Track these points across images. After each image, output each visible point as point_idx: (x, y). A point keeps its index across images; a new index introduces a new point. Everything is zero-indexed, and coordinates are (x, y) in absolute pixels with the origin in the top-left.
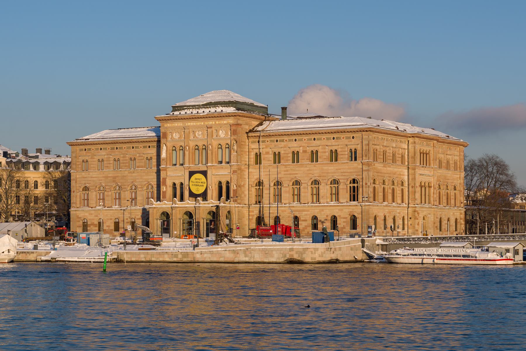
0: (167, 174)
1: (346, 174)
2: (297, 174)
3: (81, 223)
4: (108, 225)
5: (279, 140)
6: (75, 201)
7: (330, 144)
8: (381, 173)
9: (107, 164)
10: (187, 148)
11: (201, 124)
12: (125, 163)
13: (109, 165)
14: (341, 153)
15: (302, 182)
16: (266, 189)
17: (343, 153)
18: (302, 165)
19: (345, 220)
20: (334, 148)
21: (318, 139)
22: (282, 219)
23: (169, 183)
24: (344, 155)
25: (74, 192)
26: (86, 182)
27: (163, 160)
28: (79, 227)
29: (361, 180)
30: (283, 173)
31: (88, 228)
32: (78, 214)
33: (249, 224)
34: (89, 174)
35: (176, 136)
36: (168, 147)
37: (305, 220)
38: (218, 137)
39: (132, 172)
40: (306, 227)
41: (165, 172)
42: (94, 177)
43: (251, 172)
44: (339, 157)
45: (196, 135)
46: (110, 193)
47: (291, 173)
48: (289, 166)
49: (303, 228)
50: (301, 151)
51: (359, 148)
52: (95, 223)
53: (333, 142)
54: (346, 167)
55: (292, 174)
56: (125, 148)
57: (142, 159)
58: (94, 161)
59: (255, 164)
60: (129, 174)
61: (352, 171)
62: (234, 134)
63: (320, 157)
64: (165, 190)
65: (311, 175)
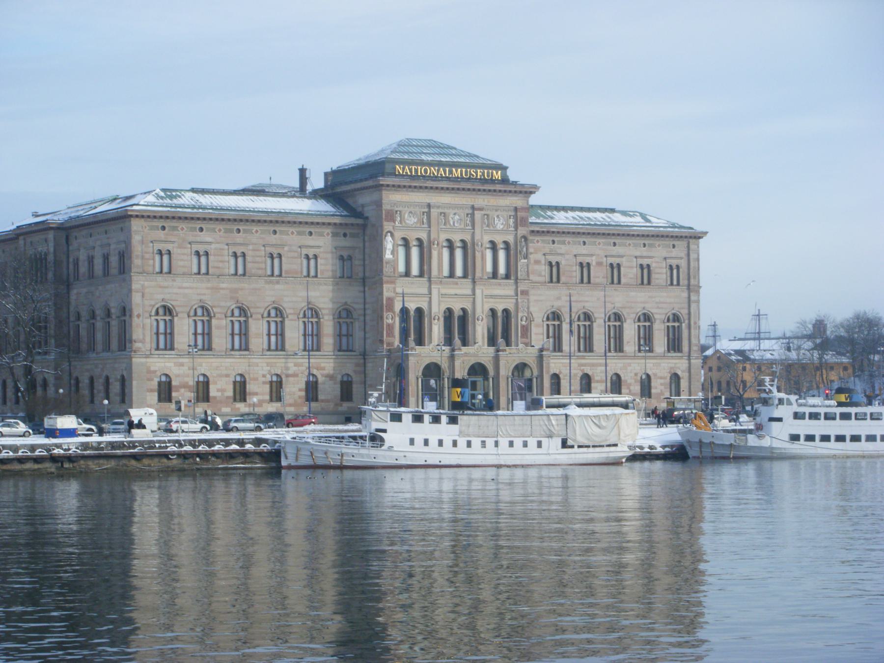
2: (587, 301)
3: (154, 384)
4: (219, 386)
6: (141, 337)
7: (638, 254)
13: (221, 265)
14: (657, 270)
15: (596, 315)
18: (597, 285)
19: (662, 381)
20: (645, 262)
23: (398, 307)
24: (660, 275)
25: (138, 316)
26: (167, 297)
27: (387, 263)
28: (152, 391)
29: (686, 317)
31: (174, 394)
35: (411, 221)
38: (492, 228)
41: (391, 286)
42: (185, 288)
44: (653, 276)
45: (449, 221)
46: (224, 322)
51: (683, 264)
53: (643, 251)
54: (665, 294)
55: (580, 301)
56: (257, 231)
57: (295, 258)
58: (184, 254)
60: (267, 286)
63: (624, 276)
64: (390, 321)
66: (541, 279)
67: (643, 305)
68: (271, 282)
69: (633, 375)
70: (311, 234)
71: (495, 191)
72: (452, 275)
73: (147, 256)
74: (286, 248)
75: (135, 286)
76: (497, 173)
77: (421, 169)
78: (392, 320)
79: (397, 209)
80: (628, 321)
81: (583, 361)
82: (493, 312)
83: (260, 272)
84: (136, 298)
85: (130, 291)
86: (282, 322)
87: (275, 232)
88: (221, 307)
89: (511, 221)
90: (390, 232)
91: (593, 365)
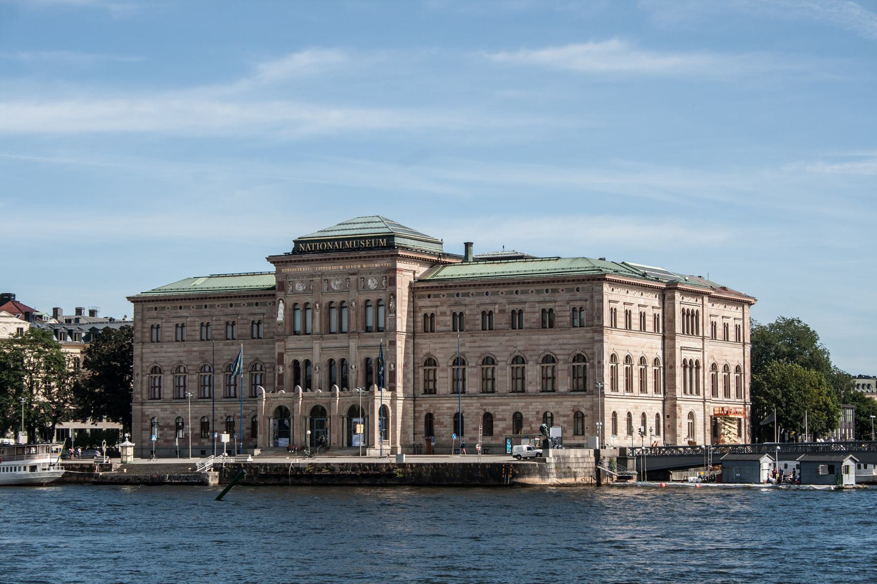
0: (285, 347)
1: (567, 347)
2: (490, 346)
5: (462, 293)
7: (541, 299)
8: (622, 345)
9: (191, 331)
10: (317, 305)
11: (339, 269)
12: (220, 330)
13: (193, 333)
14: (560, 314)
16: (443, 370)
17: (563, 314)
18: (499, 332)
20: (547, 306)
21: (523, 292)
22: (467, 418)
23: (288, 360)
25: (138, 375)
26: (157, 359)
27: (279, 325)
30: (468, 345)
32: (144, 410)
33: (414, 425)
34: (162, 347)
35: (299, 287)
36: (288, 304)
37: (504, 420)
39: (230, 344)
40: (504, 430)
42: (169, 352)
43: (418, 344)
47: (481, 345)
48: (477, 335)
49: (500, 431)
50: (497, 311)
52: (171, 424)
53: (546, 296)
54: (569, 336)
56: (218, 306)
58: (169, 327)
59: (423, 331)
60: (225, 347)
61: (577, 341)
62: (390, 285)
63: (526, 320)
64: (281, 372)
65: (511, 349)
66: (446, 328)
67: (545, 347)
68: (228, 344)
69: (535, 413)
70: (257, 304)
71: (360, 257)
73: (145, 330)
74: (239, 317)
76: (383, 241)
77: (319, 245)
79: (290, 280)
80: (530, 363)
81: (485, 401)
83: (220, 337)
84: (137, 362)
87: (231, 305)
88: (191, 365)
90: (282, 300)
91: (494, 405)
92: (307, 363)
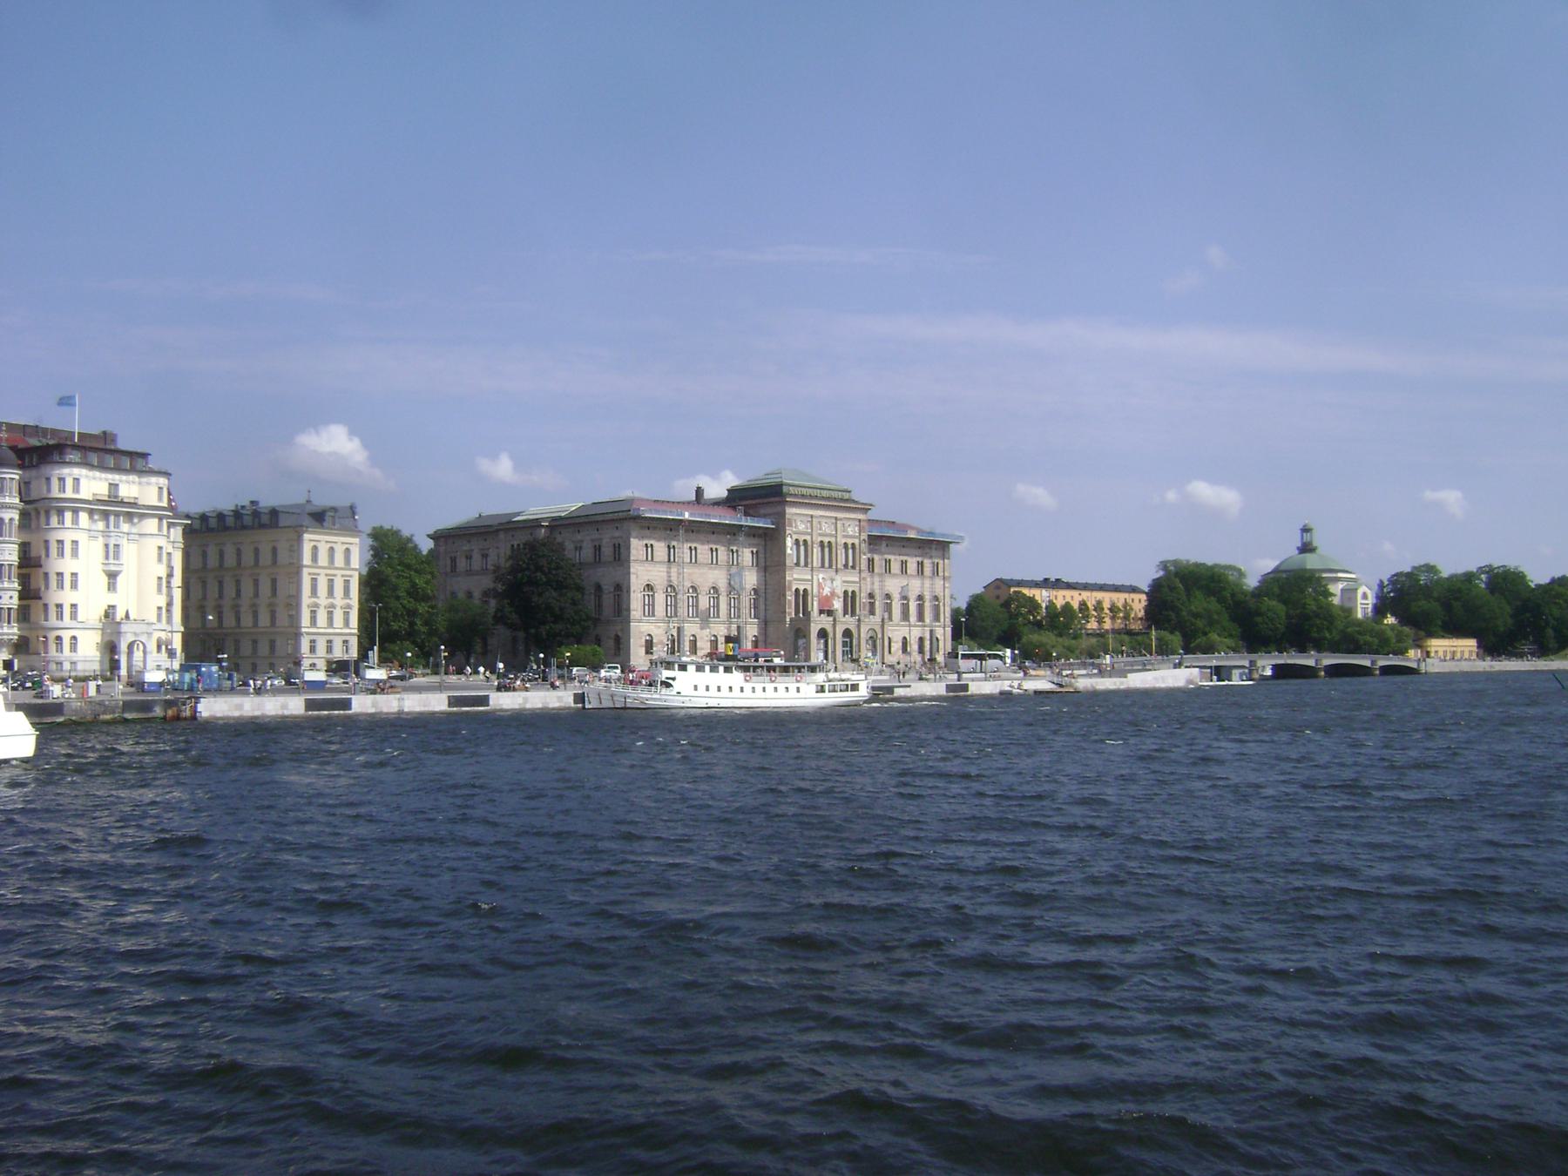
3: (643, 641)
18: (895, 575)
26: (650, 578)
37: (896, 642)
68: (711, 568)
72: (823, 566)
75: (632, 570)
78: (790, 597)
82: (846, 592)
83: (705, 561)
84: (633, 578)
85: (629, 573)
86: (718, 598)
89: (857, 529)
92: (805, 590)
